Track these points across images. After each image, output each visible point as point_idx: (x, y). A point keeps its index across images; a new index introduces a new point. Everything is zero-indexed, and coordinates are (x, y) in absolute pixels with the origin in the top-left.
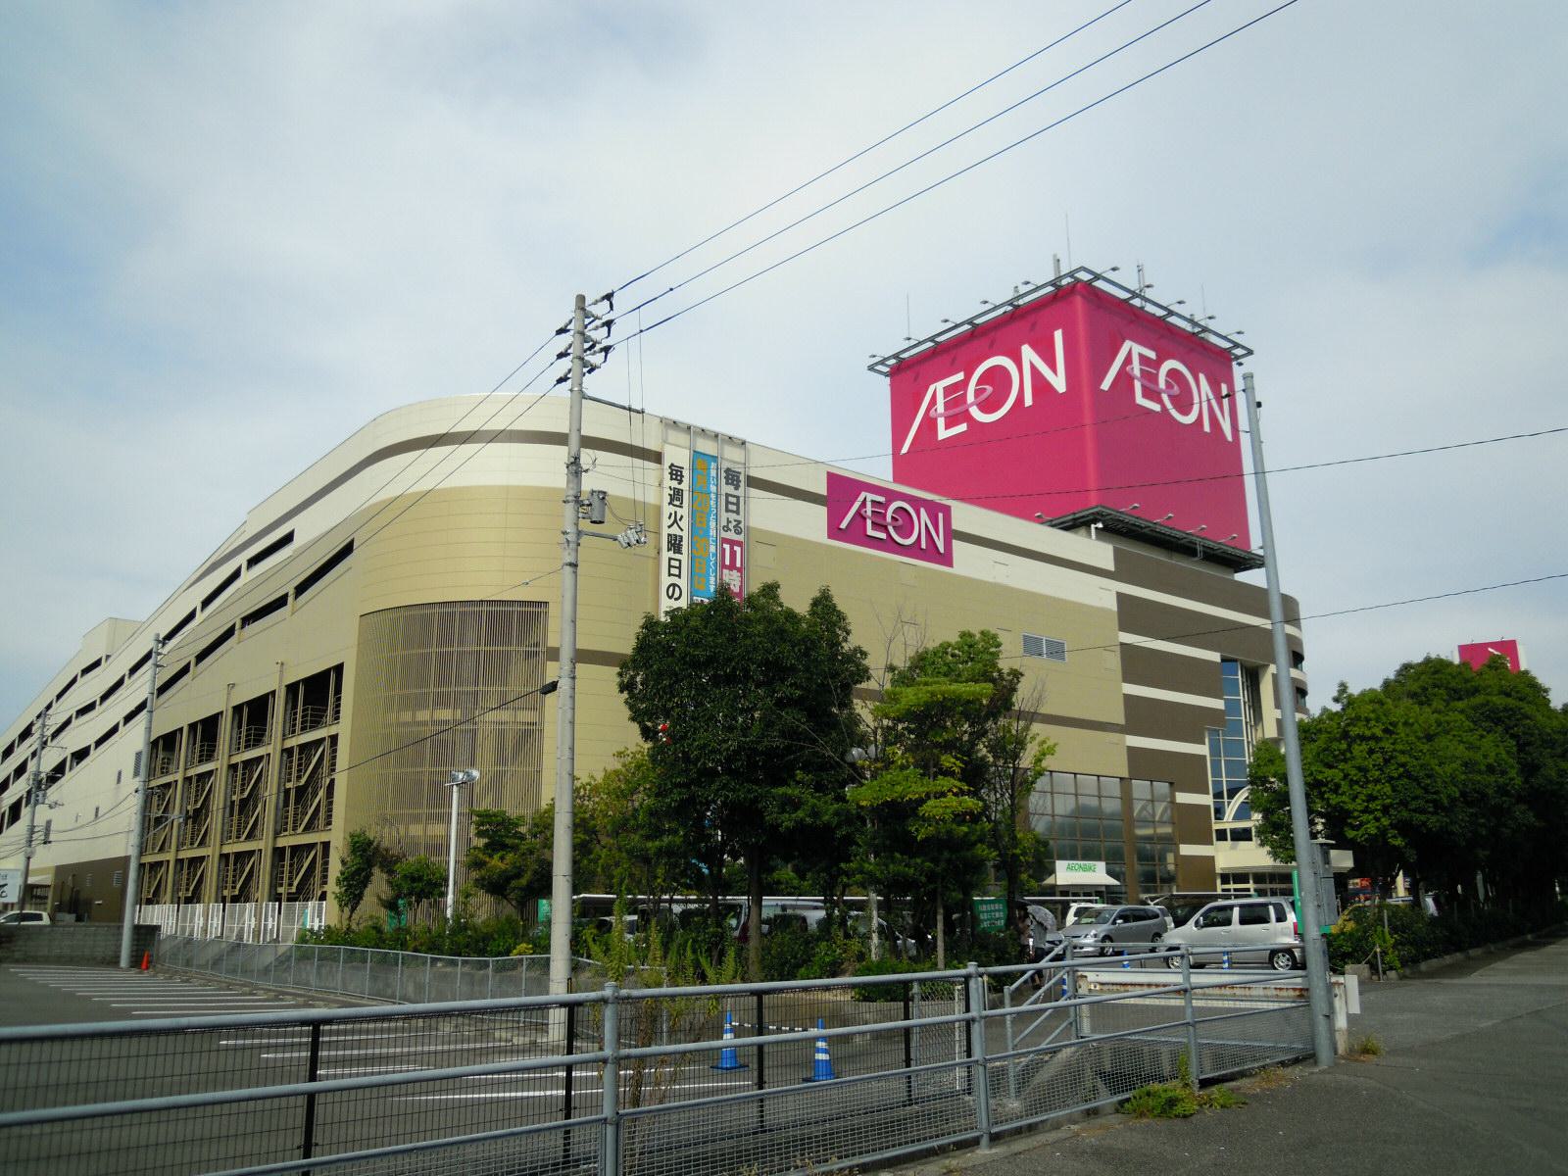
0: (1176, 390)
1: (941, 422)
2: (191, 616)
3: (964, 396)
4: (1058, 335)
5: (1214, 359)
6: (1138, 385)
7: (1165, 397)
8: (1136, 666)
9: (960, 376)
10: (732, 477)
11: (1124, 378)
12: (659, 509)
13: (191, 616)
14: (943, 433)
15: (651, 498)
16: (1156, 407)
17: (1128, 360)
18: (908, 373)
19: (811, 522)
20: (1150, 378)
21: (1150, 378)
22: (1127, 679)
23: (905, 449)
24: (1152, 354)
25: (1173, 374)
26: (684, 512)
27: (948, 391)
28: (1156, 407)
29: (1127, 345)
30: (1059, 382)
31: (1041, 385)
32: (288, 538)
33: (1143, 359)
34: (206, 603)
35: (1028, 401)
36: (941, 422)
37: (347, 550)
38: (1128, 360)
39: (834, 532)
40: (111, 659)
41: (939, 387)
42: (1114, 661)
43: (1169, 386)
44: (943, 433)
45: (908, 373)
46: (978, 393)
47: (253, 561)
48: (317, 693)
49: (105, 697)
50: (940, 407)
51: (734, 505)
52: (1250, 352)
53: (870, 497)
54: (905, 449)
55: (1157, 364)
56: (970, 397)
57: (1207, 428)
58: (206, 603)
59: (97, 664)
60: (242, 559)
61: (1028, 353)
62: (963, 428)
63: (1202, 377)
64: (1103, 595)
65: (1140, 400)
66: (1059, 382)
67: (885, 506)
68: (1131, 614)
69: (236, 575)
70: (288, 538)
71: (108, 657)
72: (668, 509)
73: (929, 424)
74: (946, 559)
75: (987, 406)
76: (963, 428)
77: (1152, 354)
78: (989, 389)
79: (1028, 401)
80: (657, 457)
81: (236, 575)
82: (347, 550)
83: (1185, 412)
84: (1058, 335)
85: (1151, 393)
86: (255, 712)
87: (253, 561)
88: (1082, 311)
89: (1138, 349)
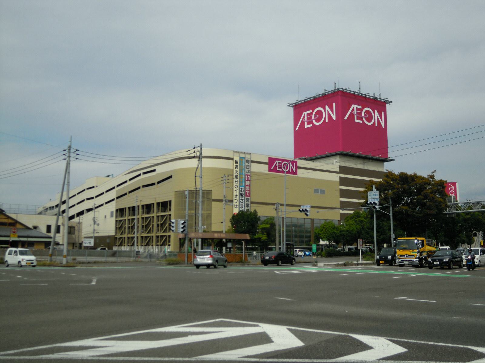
0: (367, 116)
1: (306, 123)
2: (126, 182)
3: (312, 117)
4: (334, 104)
5: (380, 105)
6: (355, 117)
7: (364, 119)
8: (343, 193)
9: (310, 111)
10: (248, 161)
11: (352, 115)
12: (233, 170)
14: (306, 126)
15: (231, 168)
16: (361, 122)
17: (353, 110)
19: (264, 169)
20: (359, 114)
21: (359, 114)
22: (341, 197)
23: (297, 129)
24: (360, 107)
25: (367, 112)
26: (238, 170)
28: (361, 122)
29: (353, 105)
30: (334, 117)
31: (330, 117)
32: (154, 171)
33: (358, 109)
34: (130, 180)
35: (327, 121)
36: (306, 123)
37: (171, 177)
38: (353, 110)
39: (270, 170)
40: (98, 187)
42: (338, 193)
43: (365, 115)
44: (306, 126)
45: (299, 108)
46: (315, 116)
47: (144, 173)
48: (165, 205)
49: (97, 197)
50: (306, 119)
51: (248, 167)
53: (278, 162)
54: (297, 129)
55: (362, 110)
56: (313, 118)
57: (376, 125)
58: (130, 180)
59: (93, 187)
60: (141, 172)
61: (327, 108)
62: (311, 125)
63: (376, 111)
64: (336, 178)
65: (356, 120)
66: (334, 117)
67: (281, 163)
68: (343, 181)
69: (139, 175)
70: (154, 171)
71: (97, 186)
72: (235, 170)
73: (303, 123)
74: (296, 173)
75: (318, 121)
76: (311, 125)
77: (360, 107)
78: (318, 116)
79: (327, 121)
80: (232, 159)
81: (139, 175)
82: (171, 177)
83: (370, 121)
84: (334, 104)
85: (359, 118)
86: (148, 208)
87: (144, 173)
88: (342, 97)
89: (356, 106)
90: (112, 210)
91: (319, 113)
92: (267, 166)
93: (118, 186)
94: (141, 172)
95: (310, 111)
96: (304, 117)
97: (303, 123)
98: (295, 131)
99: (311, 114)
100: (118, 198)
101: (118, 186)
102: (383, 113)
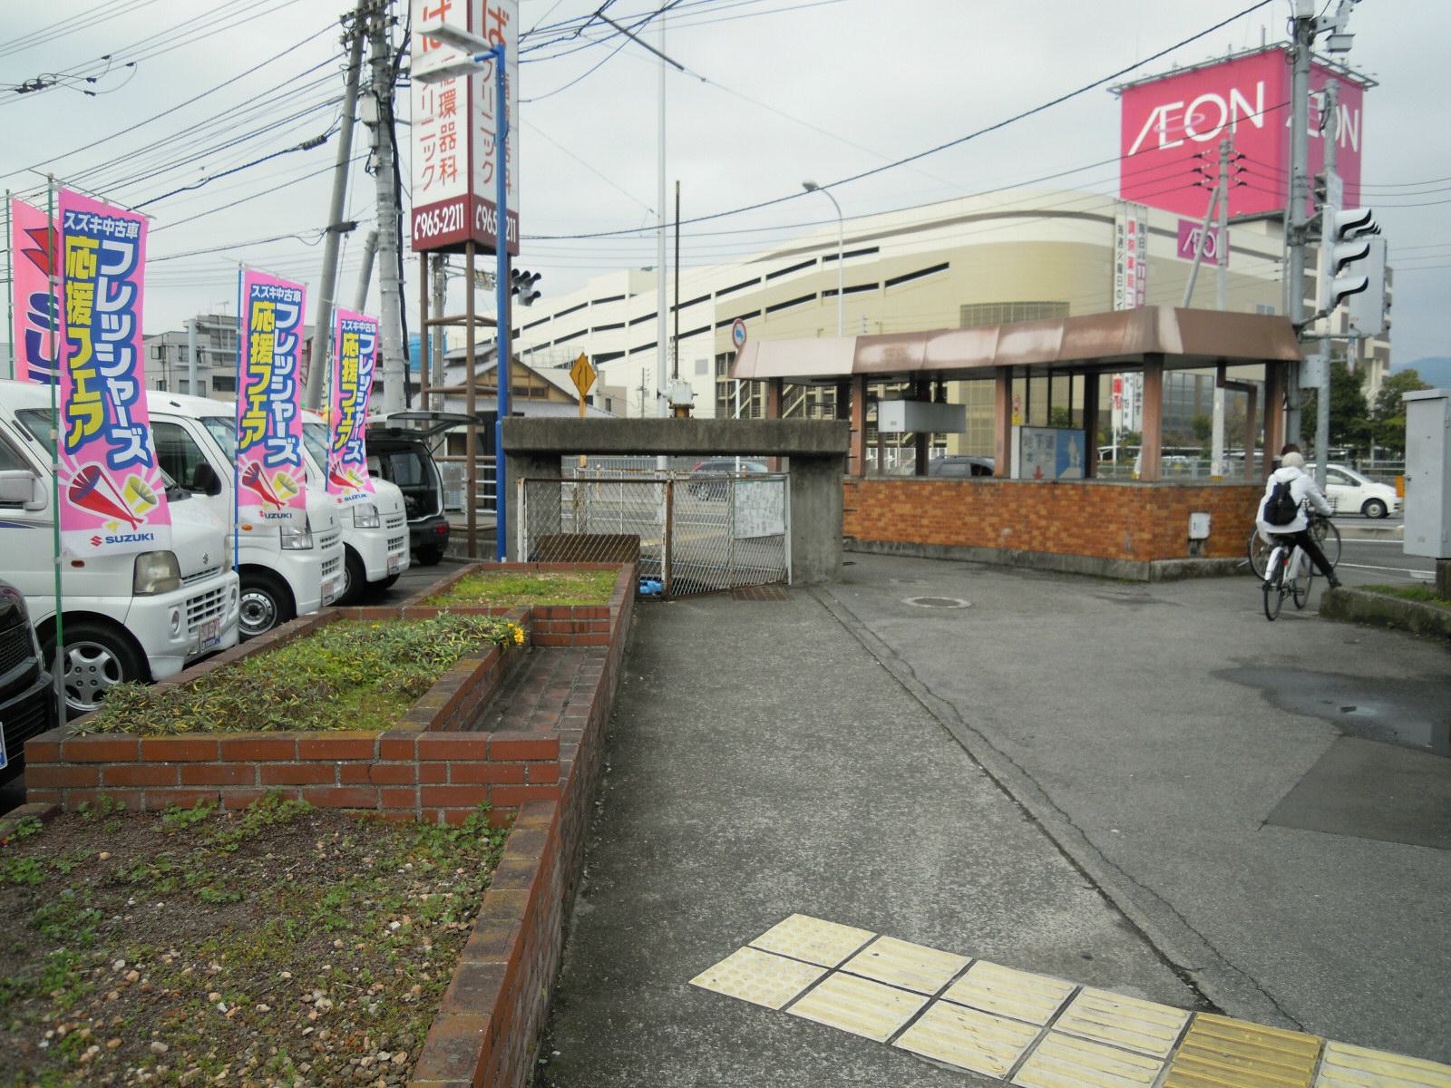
2: (758, 280)
3: (1182, 120)
4: (1260, 86)
9: (1180, 105)
12: (1113, 250)
13: (758, 280)
15: (1108, 243)
18: (1138, 98)
23: (1132, 152)
27: (1170, 114)
30: (1258, 121)
31: (1243, 118)
32: (875, 250)
34: (770, 277)
37: (945, 266)
39: (1181, 253)
40: (634, 298)
41: (1162, 111)
45: (1138, 98)
46: (1194, 119)
52: (1376, 84)
56: (1187, 121)
58: (770, 277)
61: (1236, 95)
62: (1180, 143)
66: (1258, 121)
69: (814, 262)
70: (875, 250)
71: (632, 295)
72: (1117, 250)
73: (1153, 135)
75: (1202, 129)
76: (1180, 143)
80: (1112, 221)
81: (814, 262)
82: (945, 266)
84: (1260, 86)
90: (701, 357)
91: (1211, 109)
92: (1174, 243)
93: (719, 293)
94: (818, 255)
95: (1180, 105)
96: (1157, 120)
97: (1153, 135)
98: (1124, 157)
99: (1182, 111)
100: (719, 325)
101: (719, 293)
102: (1356, 112)
